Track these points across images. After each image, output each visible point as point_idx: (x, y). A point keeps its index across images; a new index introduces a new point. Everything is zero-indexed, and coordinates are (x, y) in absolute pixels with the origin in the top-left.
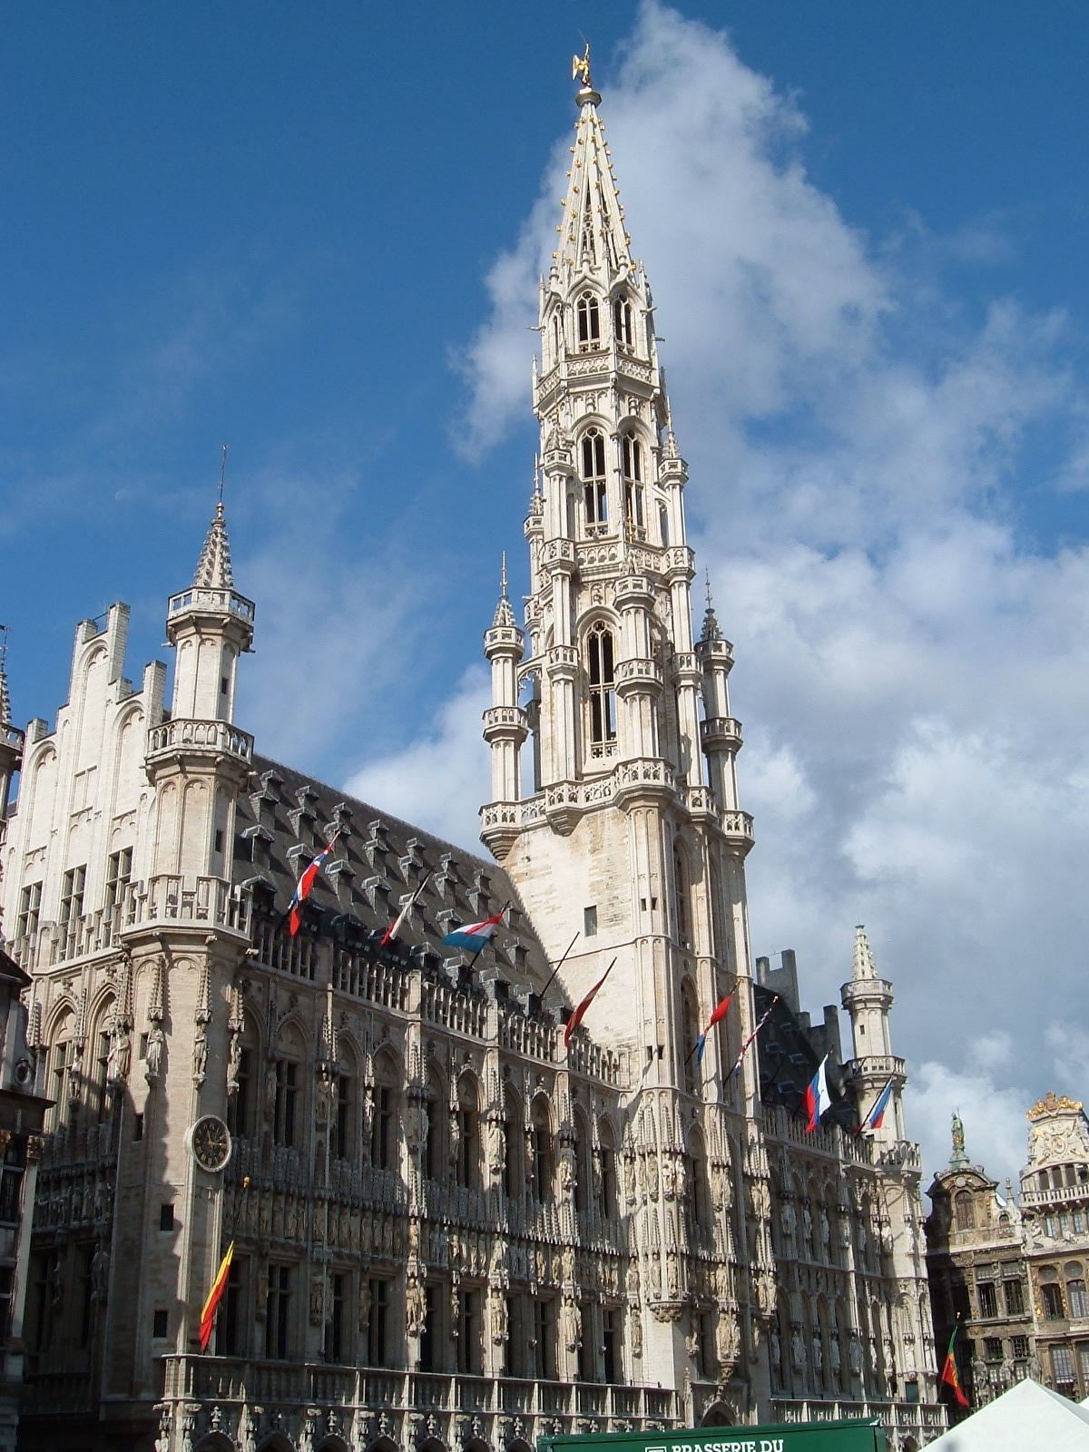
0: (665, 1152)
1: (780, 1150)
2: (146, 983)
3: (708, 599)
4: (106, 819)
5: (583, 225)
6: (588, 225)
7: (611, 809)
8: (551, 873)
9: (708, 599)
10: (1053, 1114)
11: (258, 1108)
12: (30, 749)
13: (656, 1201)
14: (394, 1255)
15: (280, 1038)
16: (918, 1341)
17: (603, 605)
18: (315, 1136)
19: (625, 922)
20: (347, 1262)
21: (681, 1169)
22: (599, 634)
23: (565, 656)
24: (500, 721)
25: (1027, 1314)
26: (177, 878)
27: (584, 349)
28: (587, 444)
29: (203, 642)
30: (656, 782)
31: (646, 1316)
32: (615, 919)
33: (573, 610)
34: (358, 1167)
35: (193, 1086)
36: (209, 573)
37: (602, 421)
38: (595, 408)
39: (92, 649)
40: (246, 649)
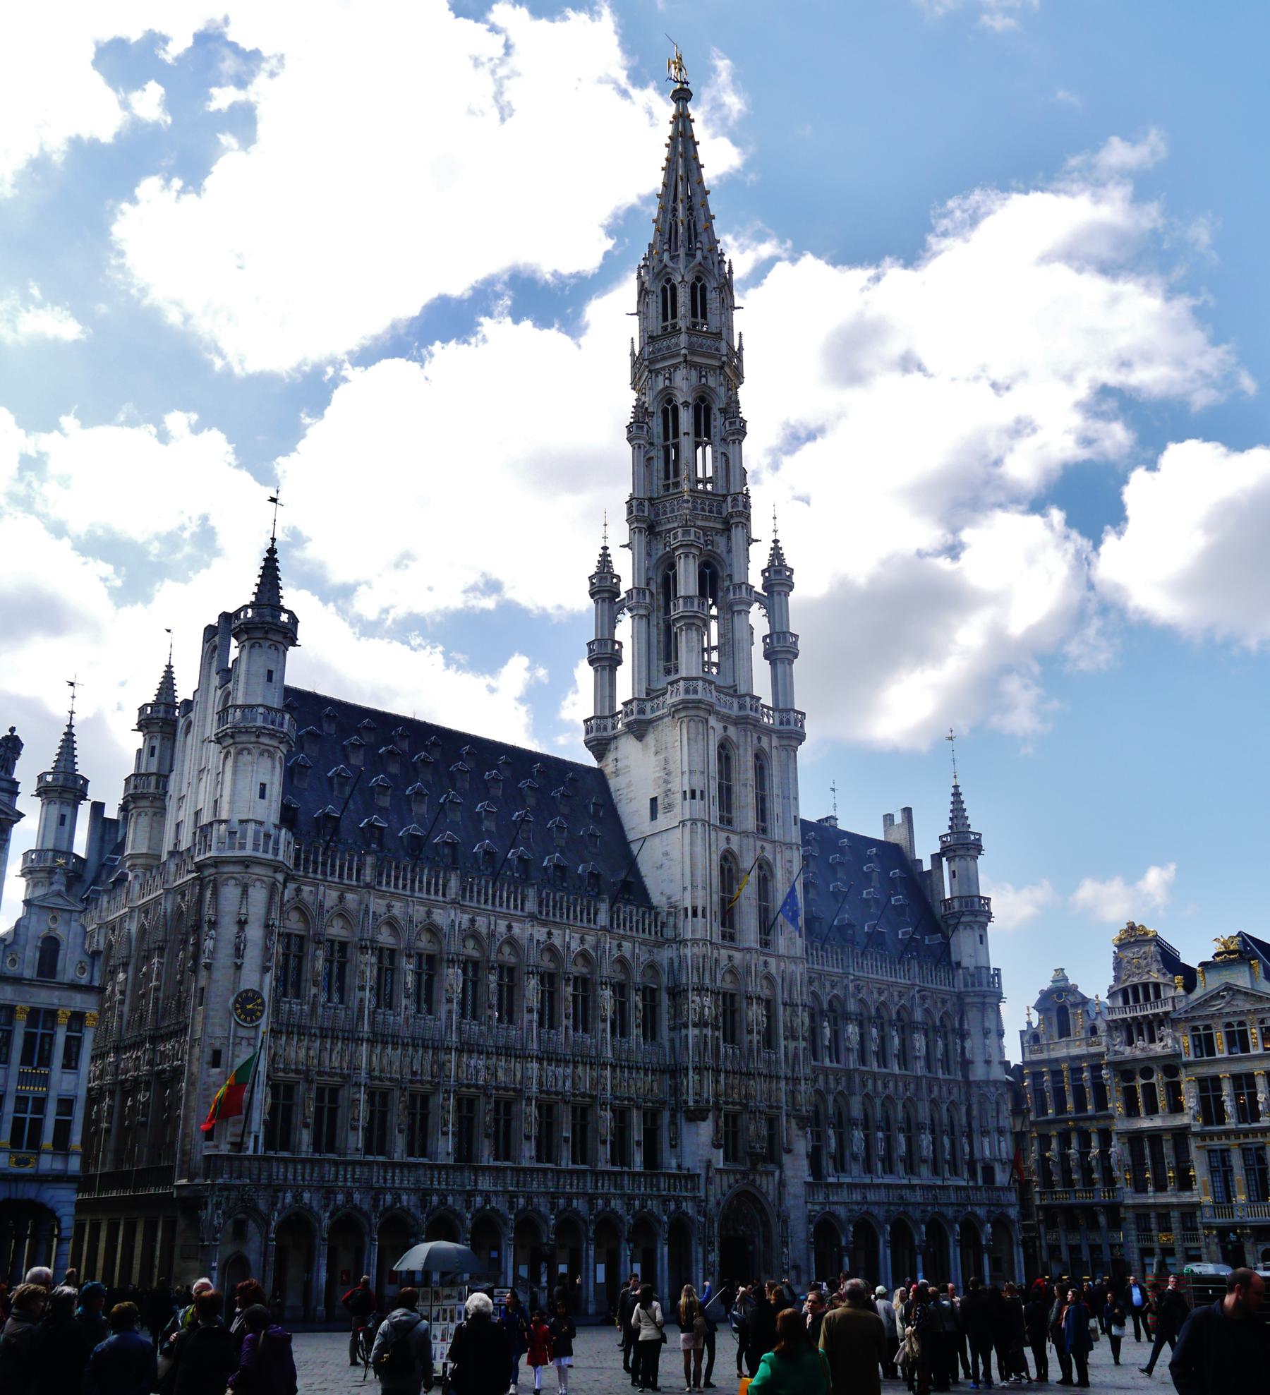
0: (693, 989)
1: (845, 981)
2: (208, 894)
3: (775, 531)
5: (670, 216)
6: (674, 215)
7: (666, 720)
9: (775, 531)
12: (182, 721)
13: (687, 1027)
14: (432, 1076)
15: (332, 926)
18: (359, 994)
19: (677, 810)
20: (388, 1083)
21: (708, 1001)
22: (671, 573)
23: (638, 594)
27: (665, 329)
28: (665, 412)
29: (252, 646)
31: (681, 1119)
32: (669, 808)
33: (649, 555)
34: (399, 1014)
37: (676, 392)
38: (670, 380)
40: (294, 645)
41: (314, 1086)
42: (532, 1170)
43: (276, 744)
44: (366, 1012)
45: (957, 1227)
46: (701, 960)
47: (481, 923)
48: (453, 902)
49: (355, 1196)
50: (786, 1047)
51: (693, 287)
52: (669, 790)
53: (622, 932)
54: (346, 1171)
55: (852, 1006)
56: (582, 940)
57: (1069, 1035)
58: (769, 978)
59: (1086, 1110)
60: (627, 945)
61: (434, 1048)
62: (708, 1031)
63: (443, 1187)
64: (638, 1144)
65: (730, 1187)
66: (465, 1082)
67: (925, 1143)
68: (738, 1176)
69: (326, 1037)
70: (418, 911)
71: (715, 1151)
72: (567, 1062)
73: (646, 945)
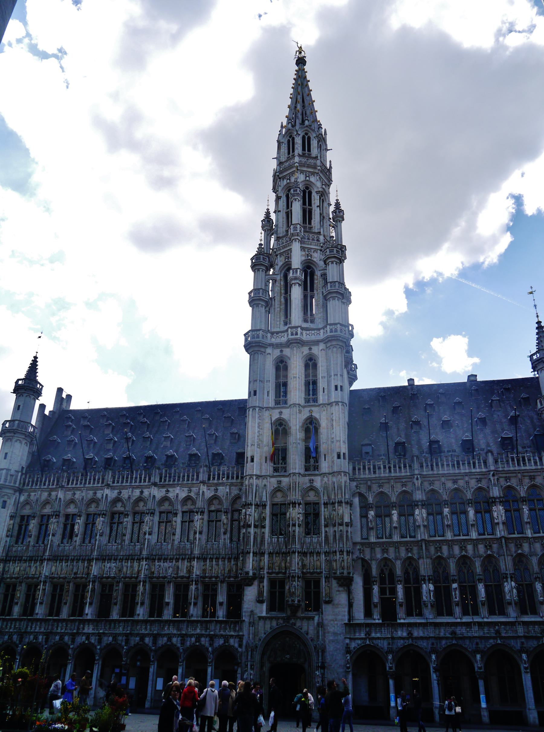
41: (24, 585)
42: (119, 621)
43: (12, 435)
44: (49, 546)
45: (524, 656)
46: (247, 487)
47: (125, 494)
48: (108, 486)
49: (14, 637)
50: (326, 532)
51: (289, 141)
53: (216, 481)
54: (11, 624)
55: (418, 496)
56: (190, 491)
58: (312, 488)
60: (220, 488)
61: (88, 560)
62: (252, 530)
63: (63, 631)
64: (221, 604)
65: (271, 628)
66: (104, 575)
67: (507, 589)
68: (281, 621)
69: (32, 560)
70: (89, 493)
71: (258, 604)
72: (171, 560)
73: (236, 486)
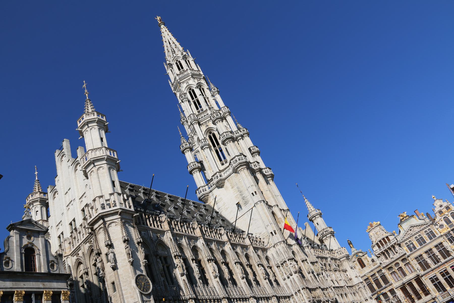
0: (289, 260)
4: (77, 200)
7: (232, 174)
8: (222, 199)
10: (373, 228)
11: (158, 273)
16: (369, 299)
17: (209, 127)
19: (250, 203)
22: (211, 134)
24: (192, 166)
25: (390, 282)
26: (102, 197)
28: (190, 93)
30: (243, 161)
32: (246, 203)
35: (129, 264)
36: (88, 109)
39: (61, 157)
52: (244, 197)
57: (365, 266)
59: (382, 286)
